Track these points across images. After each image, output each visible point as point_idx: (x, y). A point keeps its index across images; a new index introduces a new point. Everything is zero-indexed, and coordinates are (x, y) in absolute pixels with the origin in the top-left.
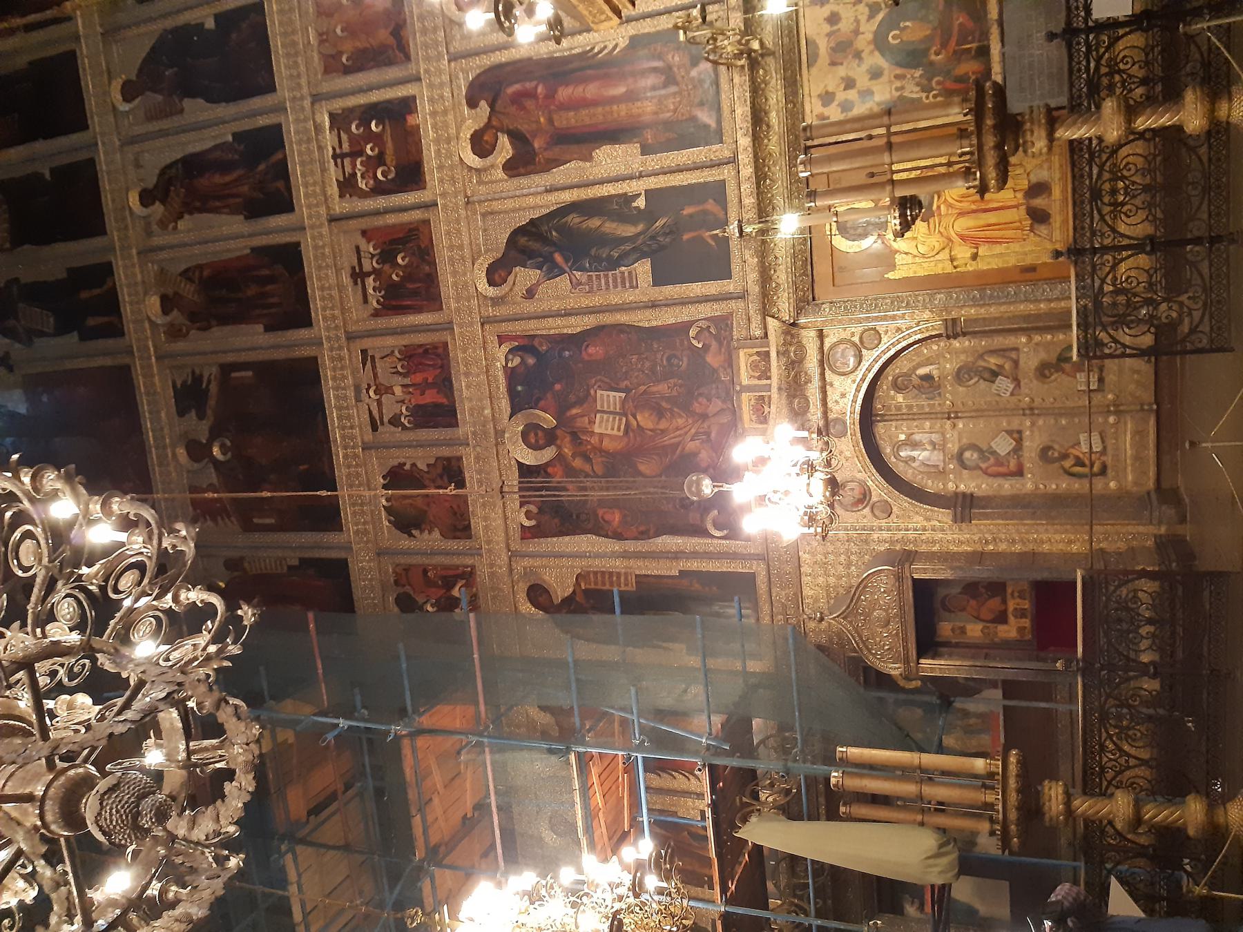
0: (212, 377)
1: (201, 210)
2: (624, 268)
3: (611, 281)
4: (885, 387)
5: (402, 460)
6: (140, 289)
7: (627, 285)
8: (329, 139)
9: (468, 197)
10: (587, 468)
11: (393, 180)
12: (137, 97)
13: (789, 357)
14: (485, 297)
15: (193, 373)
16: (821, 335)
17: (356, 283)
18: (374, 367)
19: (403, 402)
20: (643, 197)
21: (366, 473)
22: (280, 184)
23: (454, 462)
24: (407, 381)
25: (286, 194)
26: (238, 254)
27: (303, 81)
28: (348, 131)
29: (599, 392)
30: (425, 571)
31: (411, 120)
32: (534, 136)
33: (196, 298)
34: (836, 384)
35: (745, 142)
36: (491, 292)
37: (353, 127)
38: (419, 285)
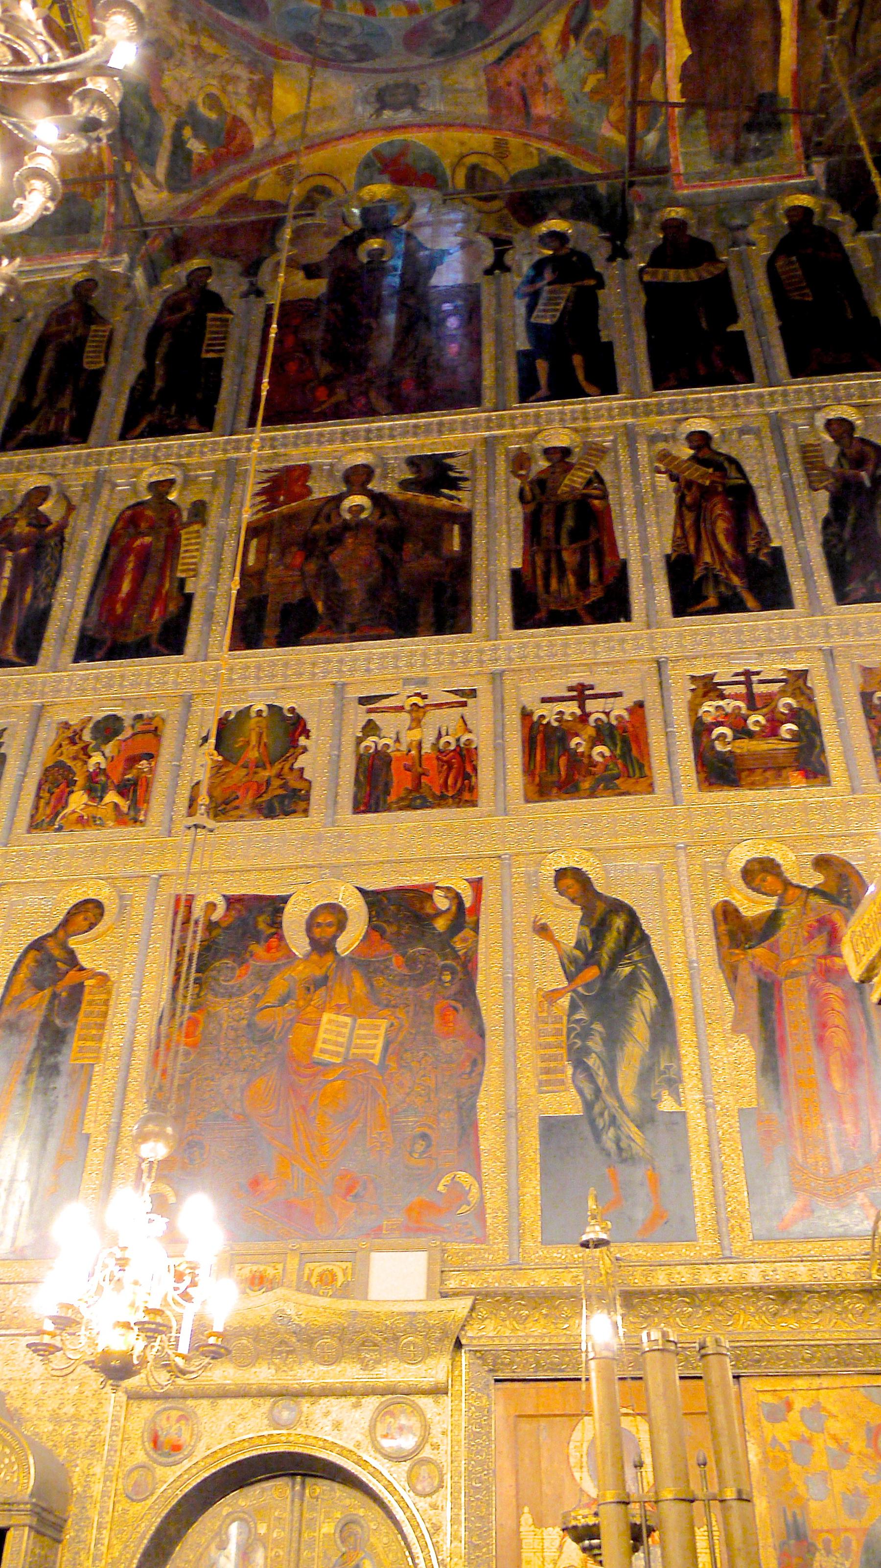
0: (455, 502)
1: (681, 502)
2: (570, 1071)
3: (553, 1051)
4: (347, 1502)
5: (313, 734)
6: (580, 424)
7: (544, 1077)
8: (774, 668)
9: (685, 848)
10: (270, 1000)
11: (713, 748)
12: (833, 437)
13: (406, 1333)
14: (539, 864)
15: (465, 479)
16: (437, 1391)
17: (571, 689)
18: (450, 705)
19: (397, 740)
20: (675, 1108)
21: (300, 686)
22: (712, 602)
23: (302, 805)
24: (427, 748)
25: (698, 608)
26: (620, 542)
27: (850, 640)
28: (783, 693)
29: (384, 1024)
30: (150, 757)
31: (795, 776)
32: (771, 949)
33: (563, 489)
34: (357, 1414)
35: (754, 1276)
36: (548, 872)
37: (789, 700)
38: (563, 773)
